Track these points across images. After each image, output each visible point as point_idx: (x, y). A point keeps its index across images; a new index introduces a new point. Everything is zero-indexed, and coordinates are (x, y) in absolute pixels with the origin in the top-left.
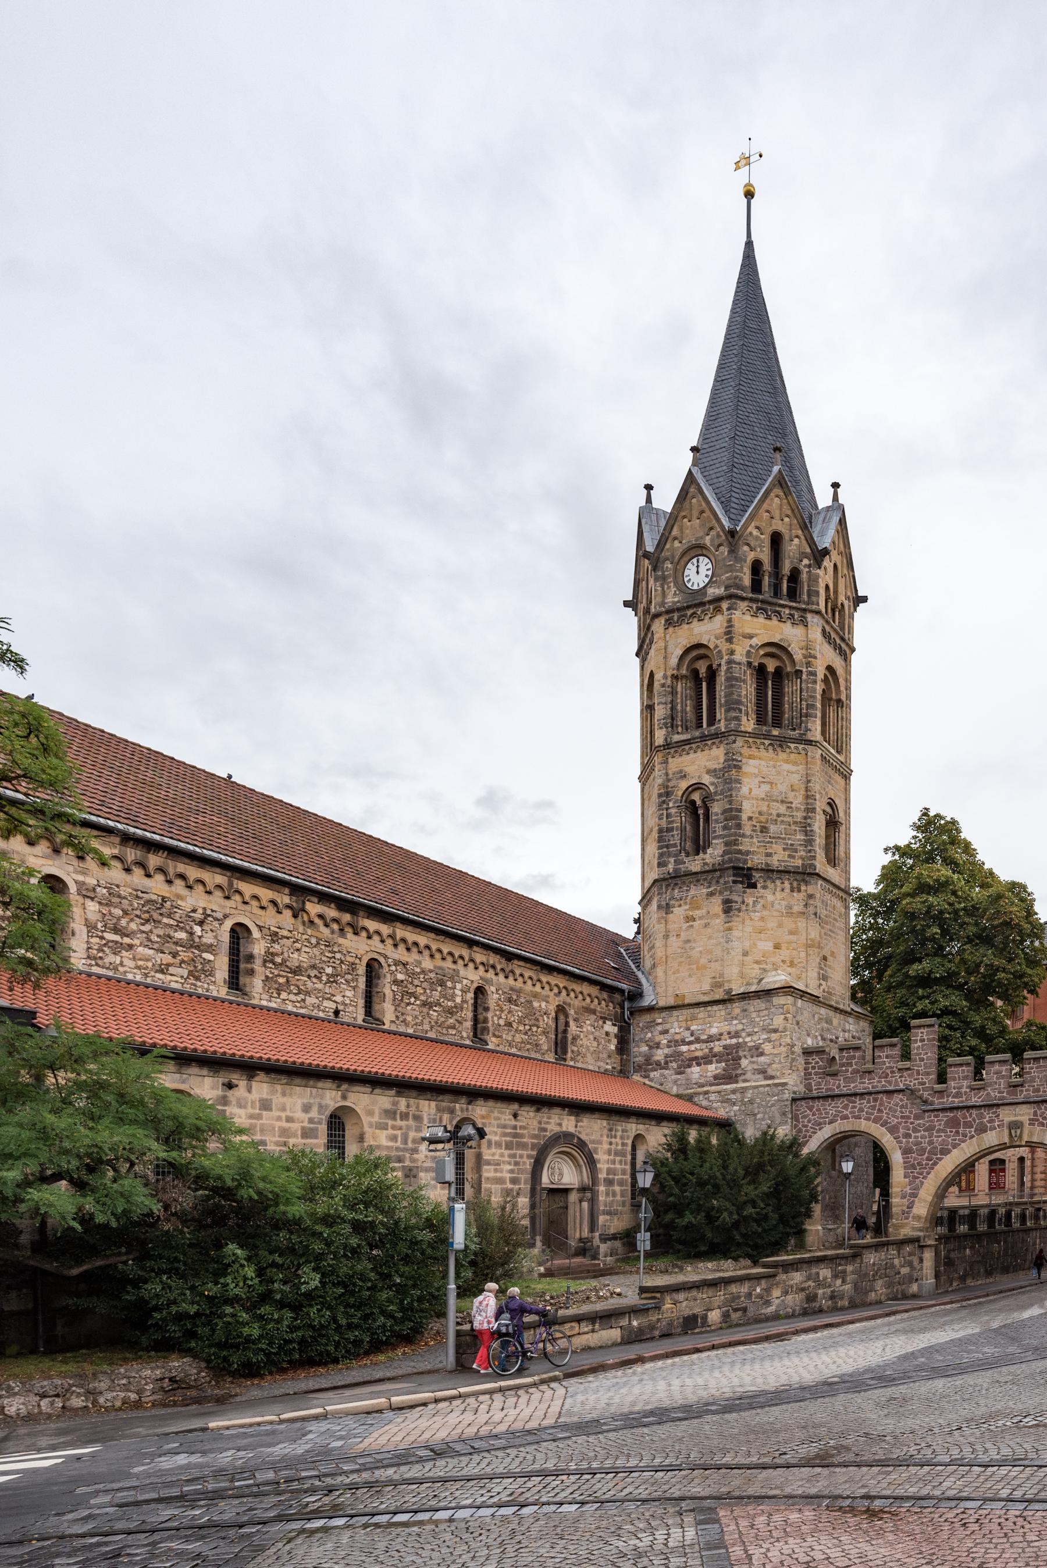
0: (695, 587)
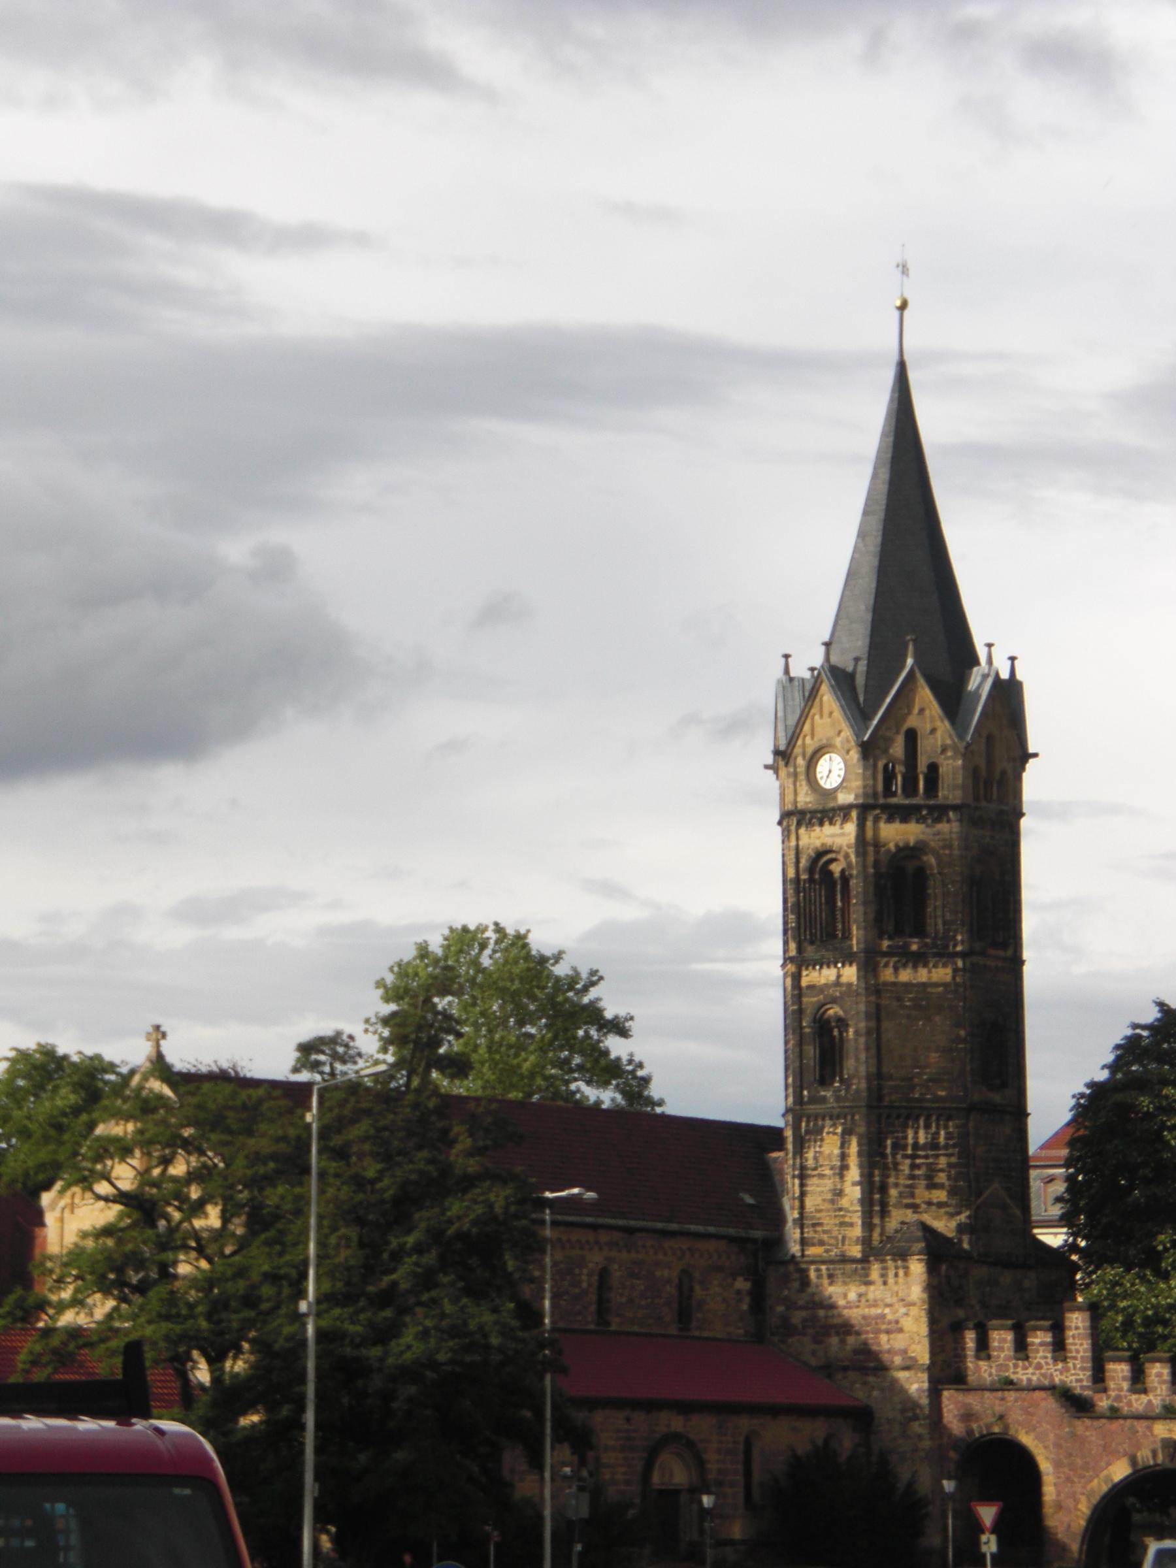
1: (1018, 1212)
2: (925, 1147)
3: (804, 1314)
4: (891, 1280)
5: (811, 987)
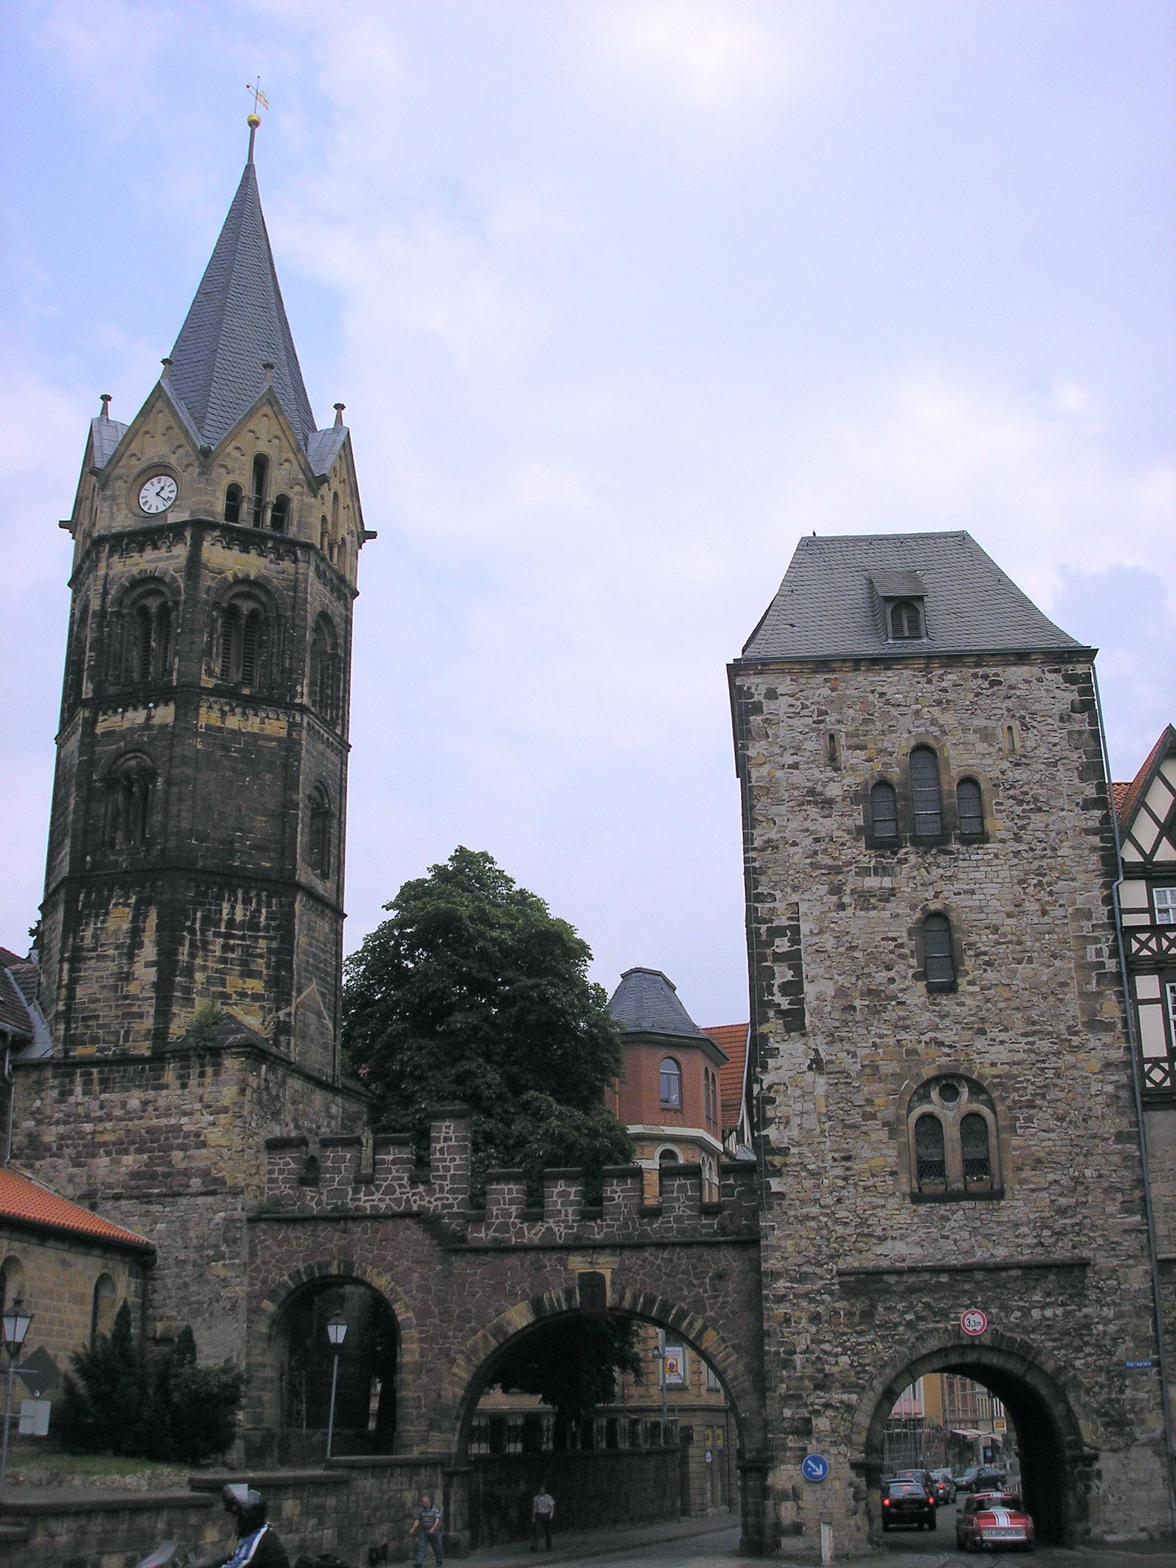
0: (153, 511)
1: (331, 1026)
2: (242, 926)
3: (61, 1129)
4: (193, 1082)
5: (109, 734)
